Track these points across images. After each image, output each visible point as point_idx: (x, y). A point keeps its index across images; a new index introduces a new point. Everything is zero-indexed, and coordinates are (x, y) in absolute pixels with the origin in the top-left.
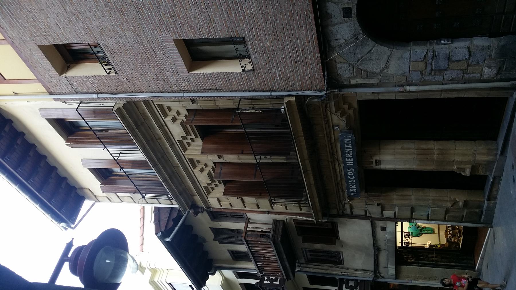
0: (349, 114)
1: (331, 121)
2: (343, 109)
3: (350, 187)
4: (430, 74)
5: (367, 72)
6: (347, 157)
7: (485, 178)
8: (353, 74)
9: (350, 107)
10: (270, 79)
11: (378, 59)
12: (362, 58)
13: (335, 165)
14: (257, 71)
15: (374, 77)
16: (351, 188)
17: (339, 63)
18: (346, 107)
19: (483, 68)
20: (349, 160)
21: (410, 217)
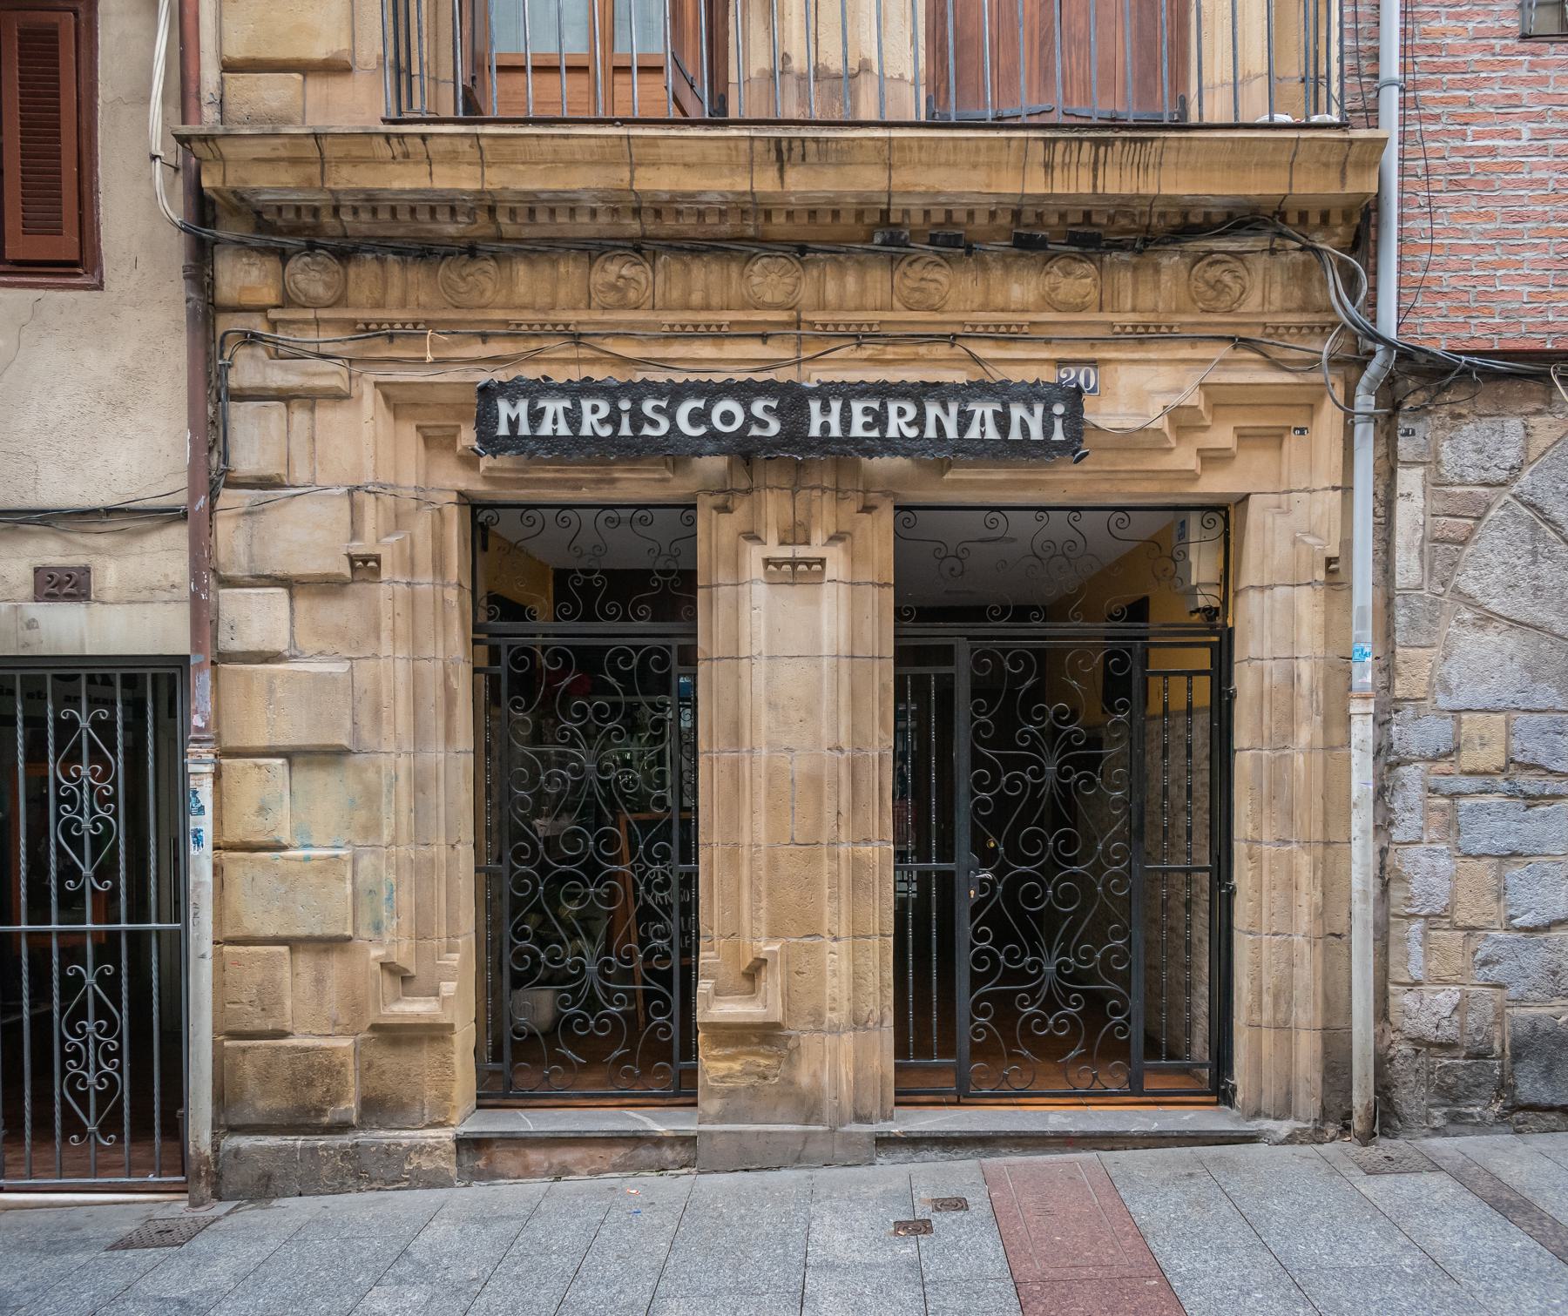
0: (1170, 450)
1: (1136, 356)
2: (1208, 423)
3: (586, 405)
4: (1434, 791)
5: (1467, 538)
6: (884, 406)
7: (684, 1091)
8: (1457, 479)
9: (1213, 458)
10: (1471, 105)
11: (1537, 588)
12: (1547, 521)
13: (765, 343)
14: (1522, 53)
15: (1432, 569)
16: (577, 406)
17: (1526, 427)
18: (1222, 436)
19: (1456, 983)
20: (858, 419)
21: (230, 742)
